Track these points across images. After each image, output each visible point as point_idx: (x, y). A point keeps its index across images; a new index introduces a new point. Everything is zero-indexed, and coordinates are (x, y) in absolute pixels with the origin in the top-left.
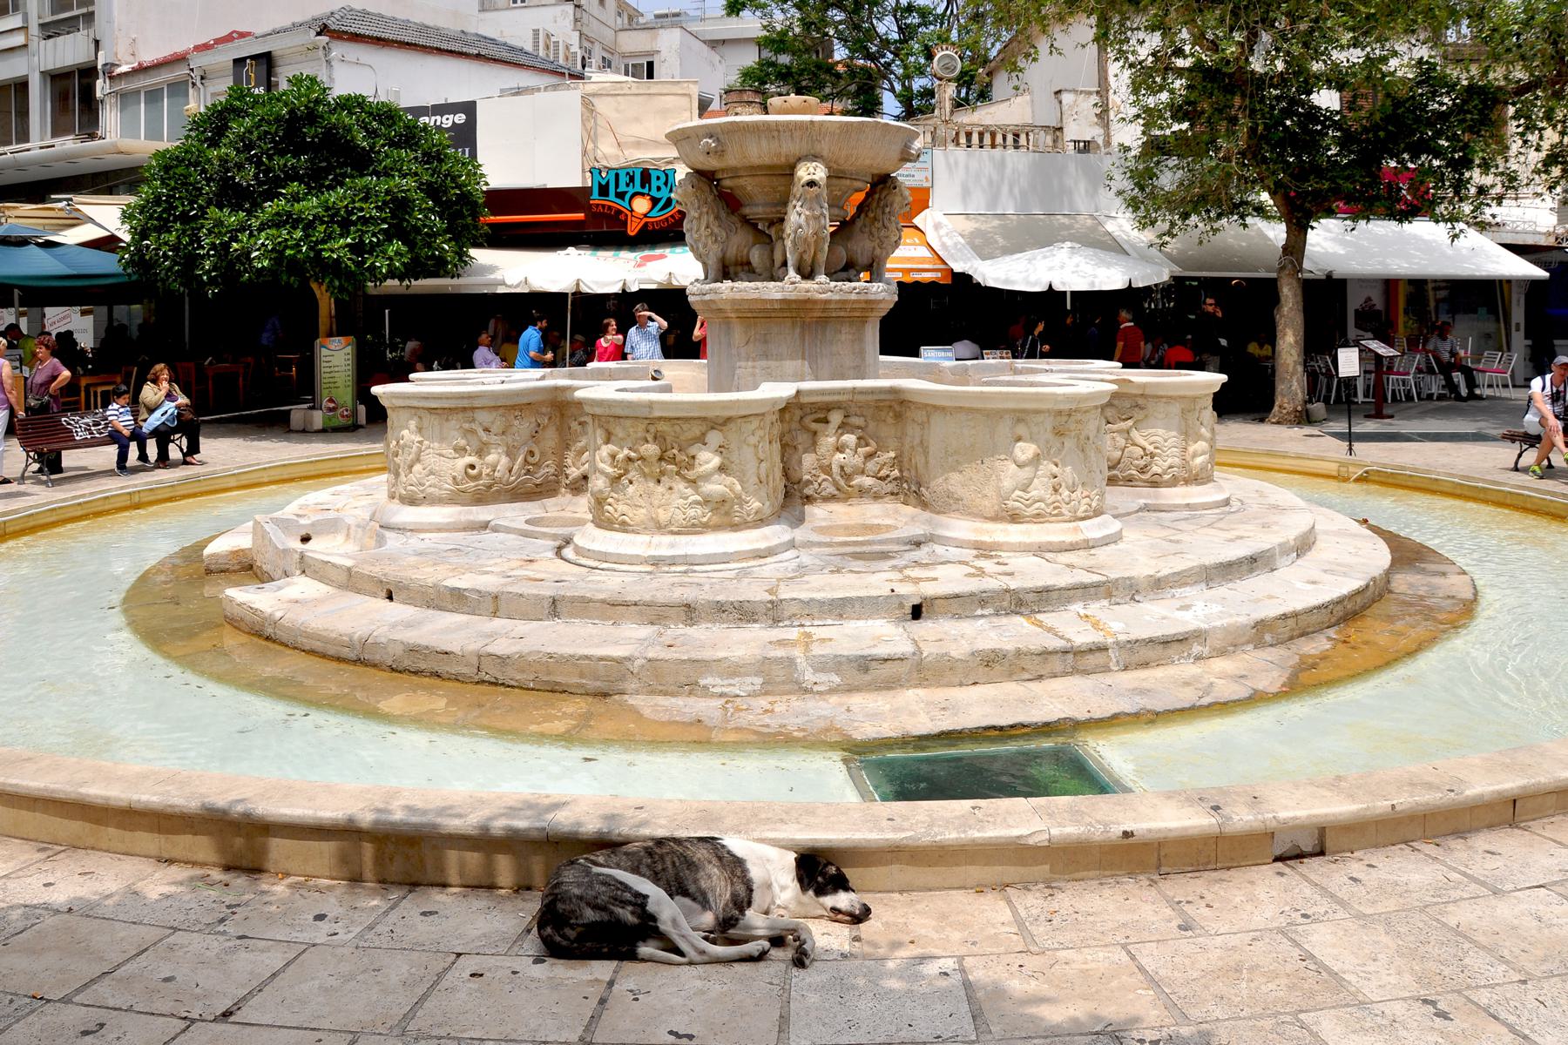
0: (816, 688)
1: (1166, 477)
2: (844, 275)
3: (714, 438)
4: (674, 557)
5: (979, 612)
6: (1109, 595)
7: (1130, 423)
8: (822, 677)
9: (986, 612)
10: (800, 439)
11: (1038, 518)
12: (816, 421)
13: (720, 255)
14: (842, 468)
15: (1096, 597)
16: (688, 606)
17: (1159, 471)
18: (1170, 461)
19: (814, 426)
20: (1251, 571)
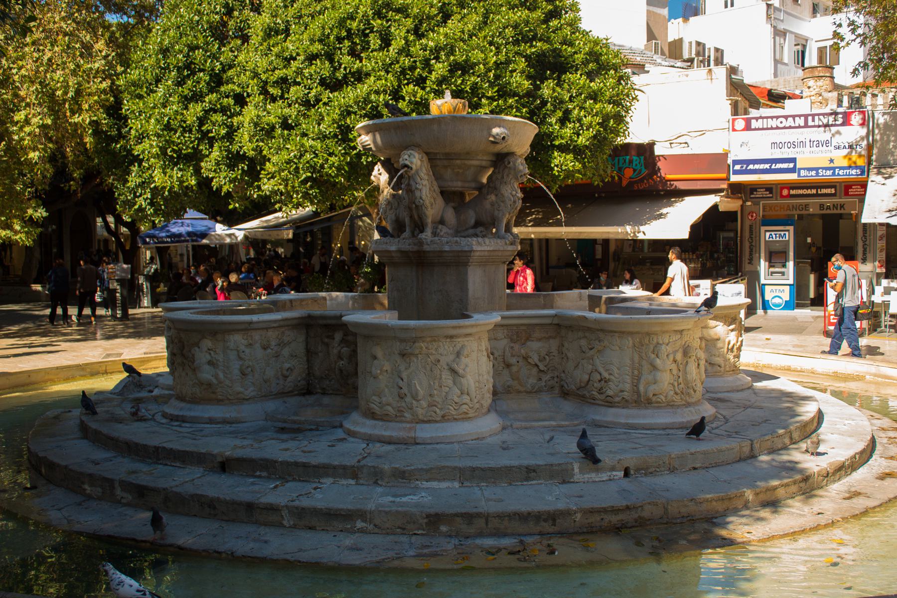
0: (123, 501)
1: (617, 399)
2: (471, 231)
3: (207, 343)
4: (178, 416)
5: (258, 473)
6: (355, 476)
7: (592, 352)
8: (125, 495)
9: (264, 474)
10: (320, 348)
11: (384, 418)
12: (328, 337)
13: (394, 218)
14: (341, 371)
15: (345, 476)
16: (127, 443)
17: (610, 392)
18: (621, 386)
19: (326, 340)
20: (528, 479)
